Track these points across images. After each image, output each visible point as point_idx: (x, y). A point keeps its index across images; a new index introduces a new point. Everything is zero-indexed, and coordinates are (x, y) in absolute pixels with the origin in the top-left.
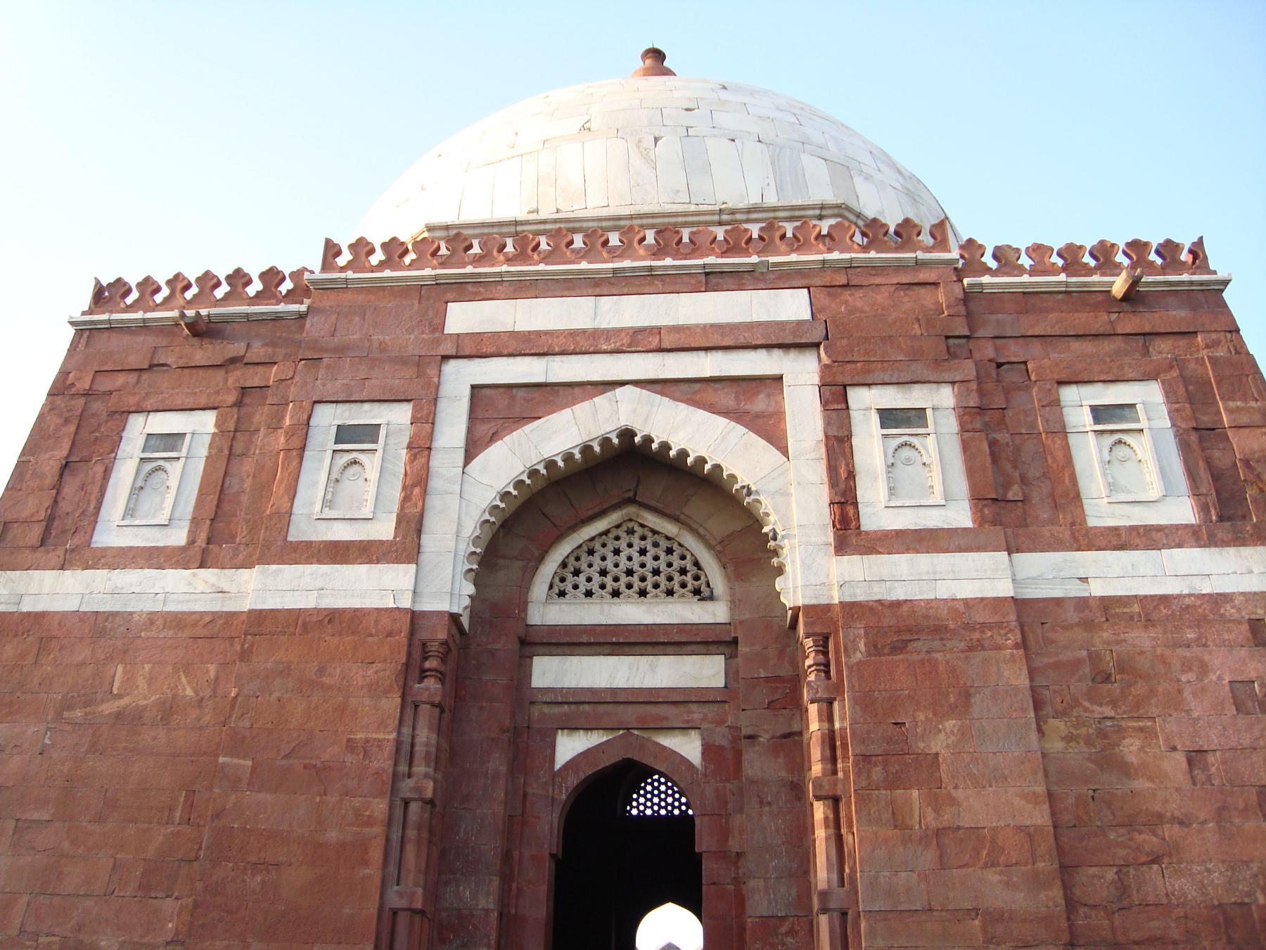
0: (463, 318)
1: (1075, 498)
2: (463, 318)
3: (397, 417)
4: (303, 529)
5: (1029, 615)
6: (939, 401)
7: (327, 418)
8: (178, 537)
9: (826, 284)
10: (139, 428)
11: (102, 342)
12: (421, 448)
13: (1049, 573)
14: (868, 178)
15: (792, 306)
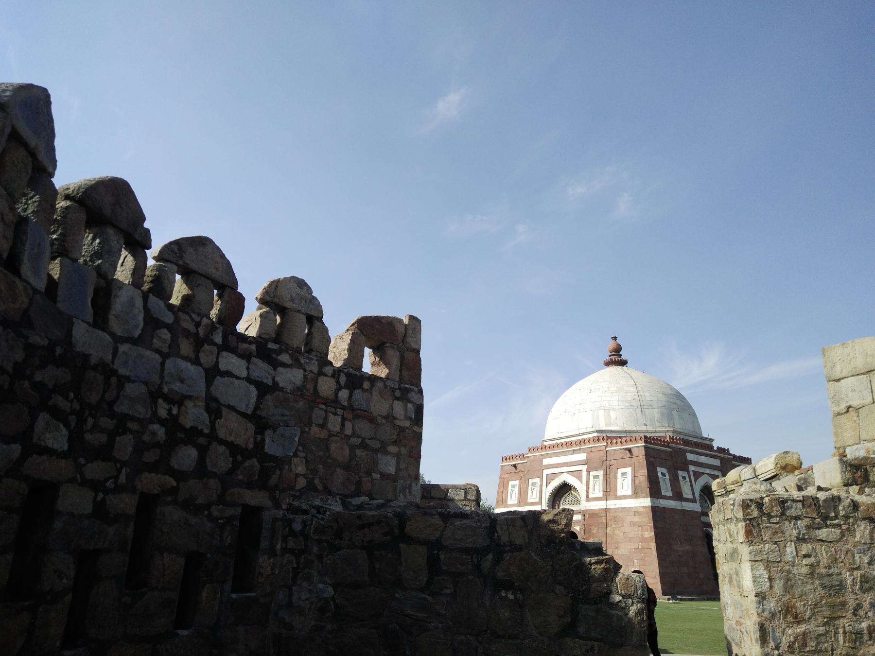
0: (546, 461)
1: (616, 490)
2: (546, 461)
3: (537, 480)
4: (530, 500)
5: (606, 510)
6: (601, 473)
7: (531, 481)
8: (516, 502)
9: (590, 451)
10: (511, 483)
11: (506, 468)
12: (541, 486)
13: (612, 504)
14: (614, 410)
15: (583, 456)
